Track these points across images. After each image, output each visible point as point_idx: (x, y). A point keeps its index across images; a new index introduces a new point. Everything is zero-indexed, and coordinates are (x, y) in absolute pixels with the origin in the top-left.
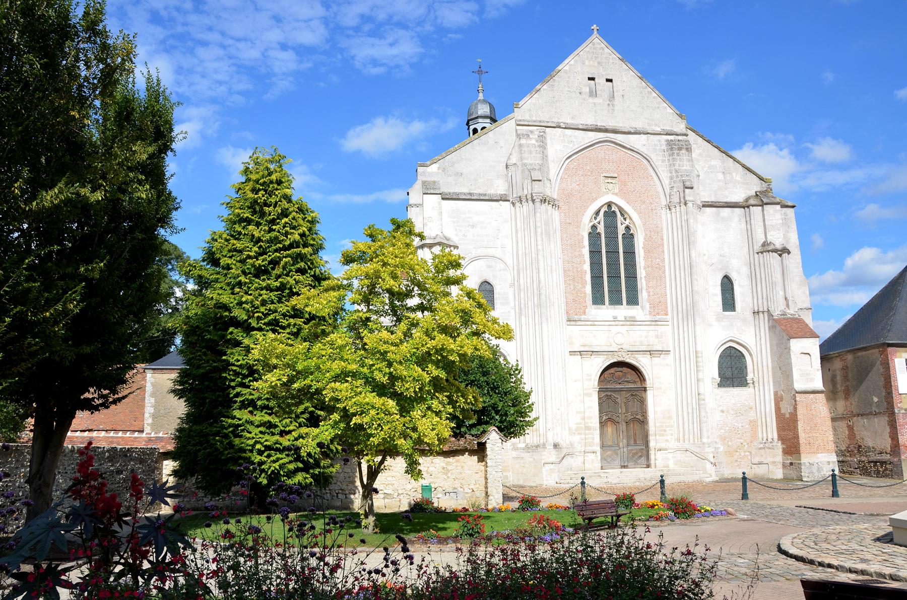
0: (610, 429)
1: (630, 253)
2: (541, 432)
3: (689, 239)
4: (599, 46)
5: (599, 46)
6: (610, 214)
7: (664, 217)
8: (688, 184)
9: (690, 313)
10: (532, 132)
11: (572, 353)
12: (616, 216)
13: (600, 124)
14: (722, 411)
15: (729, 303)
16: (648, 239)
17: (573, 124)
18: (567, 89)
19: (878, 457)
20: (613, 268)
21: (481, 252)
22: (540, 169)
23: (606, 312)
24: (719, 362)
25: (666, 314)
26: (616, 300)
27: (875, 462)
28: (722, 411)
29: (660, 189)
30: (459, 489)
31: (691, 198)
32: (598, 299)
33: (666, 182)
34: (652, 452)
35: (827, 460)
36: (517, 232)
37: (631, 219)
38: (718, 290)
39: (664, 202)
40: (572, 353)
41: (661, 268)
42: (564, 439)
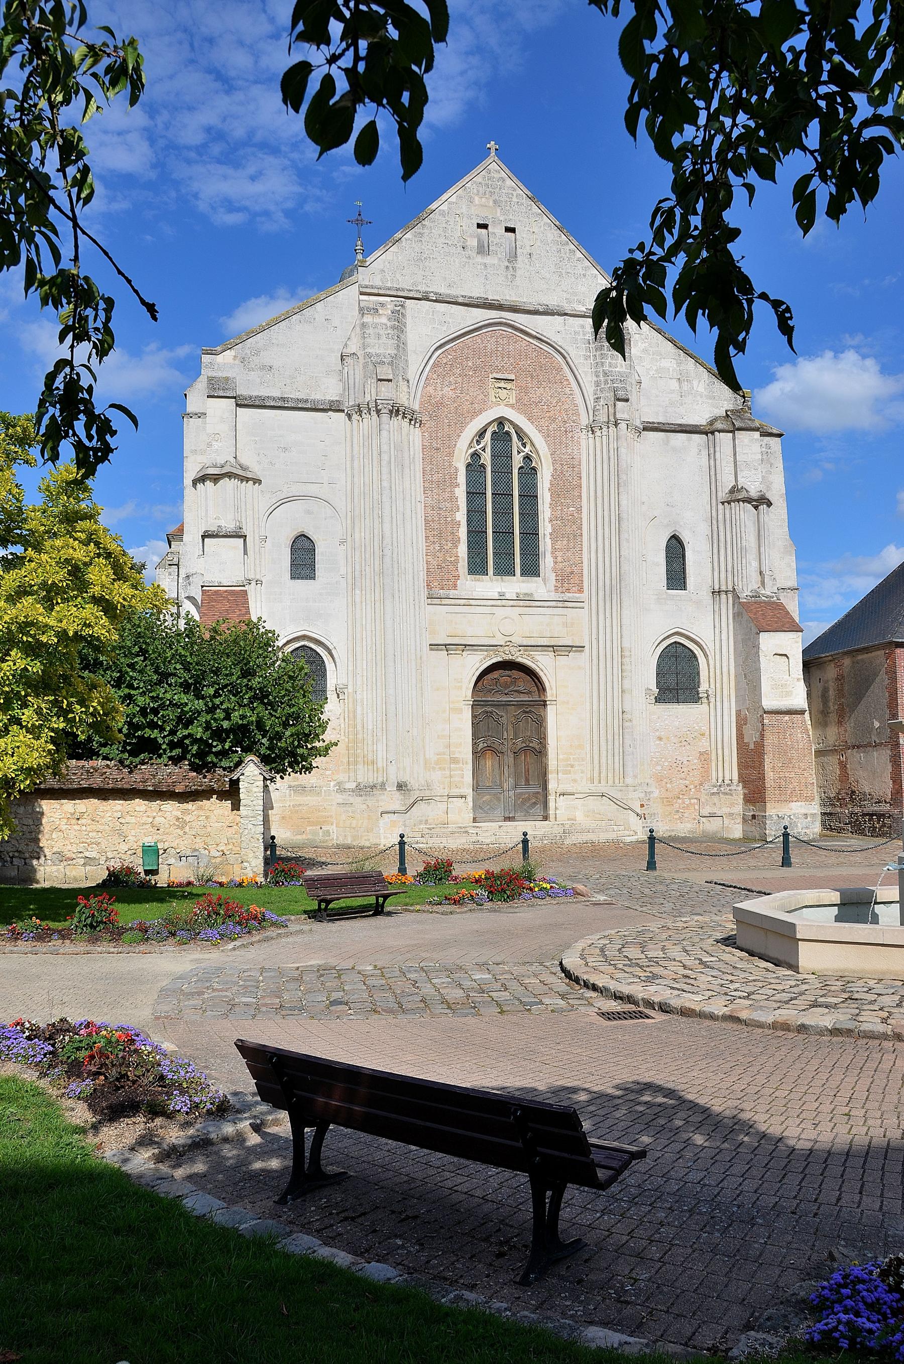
0: (489, 763)
1: (530, 498)
2: (380, 765)
3: (618, 478)
4: (496, 176)
5: (496, 176)
6: (502, 434)
7: (583, 443)
8: (621, 394)
9: (615, 590)
10: (382, 305)
11: (434, 646)
12: (511, 440)
13: (492, 296)
14: (660, 739)
15: (677, 577)
16: (557, 476)
17: (448, 295)
18: (443, 240)
19: (875, 808)
20: (502, 520)
21: (296, 490)
22: (391, 364)
23: (489, 586)
24: (658, 665)
25: (581, 591)
26: (505, 569)
27: (872, 815)
29: (579, 400)
30: (203, 851)
31: (625, 416)
32: (477, 567)
33: (589, 390)
34: (551, 798)
35: (804, 811)
36: (352, 460)
37: (533, 444)
39: (584, 421)
40: (434, 646)
42: (416, 777)
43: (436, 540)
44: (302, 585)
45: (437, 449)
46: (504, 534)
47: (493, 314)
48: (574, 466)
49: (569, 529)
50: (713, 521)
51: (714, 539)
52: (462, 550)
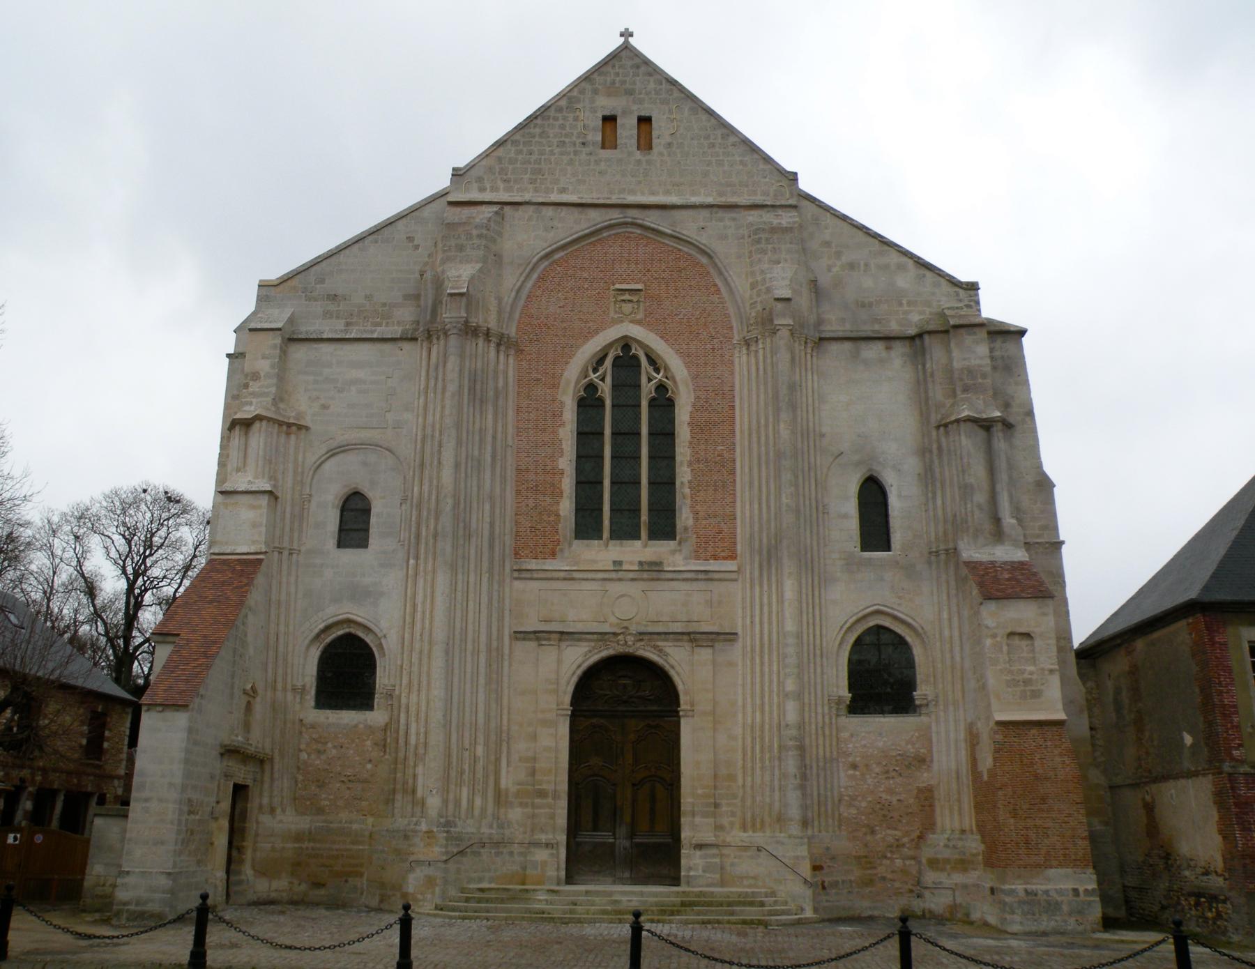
1: (664, 436)
6: (626, 361)
12: (639, 366)
14: (854, 766)
23: (602, 553)
26: (625, 531)
27: (1198, 895)
28: (854, 766)
37: (667, 369)
38: (851, 507)
41: (728, 465)
43: (529, 494)
44: (350, 556)
45: (538, 380)
46: (625, 484)
47: (615, 215)
48: (727, 395)
49: (719, 474)
50: (923, 452)
51: (928, 478)
52: (567, 507)
